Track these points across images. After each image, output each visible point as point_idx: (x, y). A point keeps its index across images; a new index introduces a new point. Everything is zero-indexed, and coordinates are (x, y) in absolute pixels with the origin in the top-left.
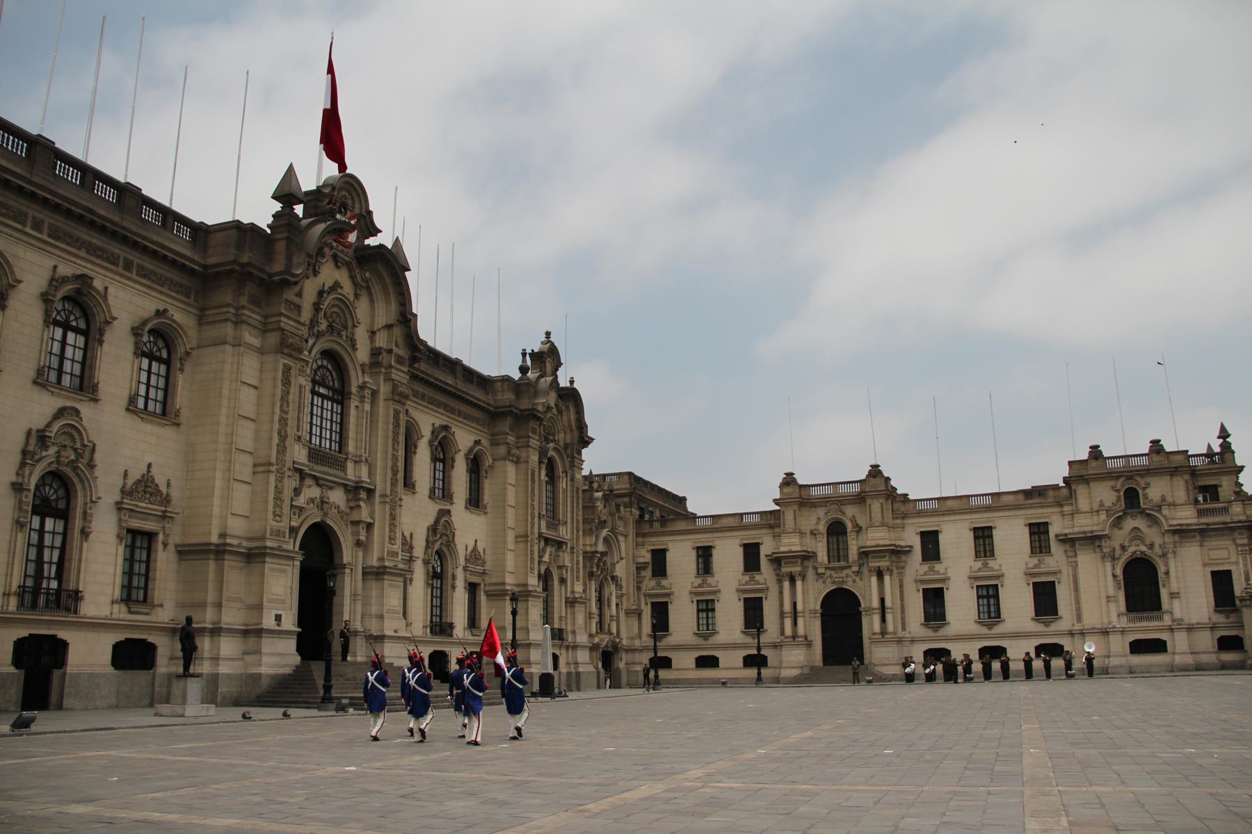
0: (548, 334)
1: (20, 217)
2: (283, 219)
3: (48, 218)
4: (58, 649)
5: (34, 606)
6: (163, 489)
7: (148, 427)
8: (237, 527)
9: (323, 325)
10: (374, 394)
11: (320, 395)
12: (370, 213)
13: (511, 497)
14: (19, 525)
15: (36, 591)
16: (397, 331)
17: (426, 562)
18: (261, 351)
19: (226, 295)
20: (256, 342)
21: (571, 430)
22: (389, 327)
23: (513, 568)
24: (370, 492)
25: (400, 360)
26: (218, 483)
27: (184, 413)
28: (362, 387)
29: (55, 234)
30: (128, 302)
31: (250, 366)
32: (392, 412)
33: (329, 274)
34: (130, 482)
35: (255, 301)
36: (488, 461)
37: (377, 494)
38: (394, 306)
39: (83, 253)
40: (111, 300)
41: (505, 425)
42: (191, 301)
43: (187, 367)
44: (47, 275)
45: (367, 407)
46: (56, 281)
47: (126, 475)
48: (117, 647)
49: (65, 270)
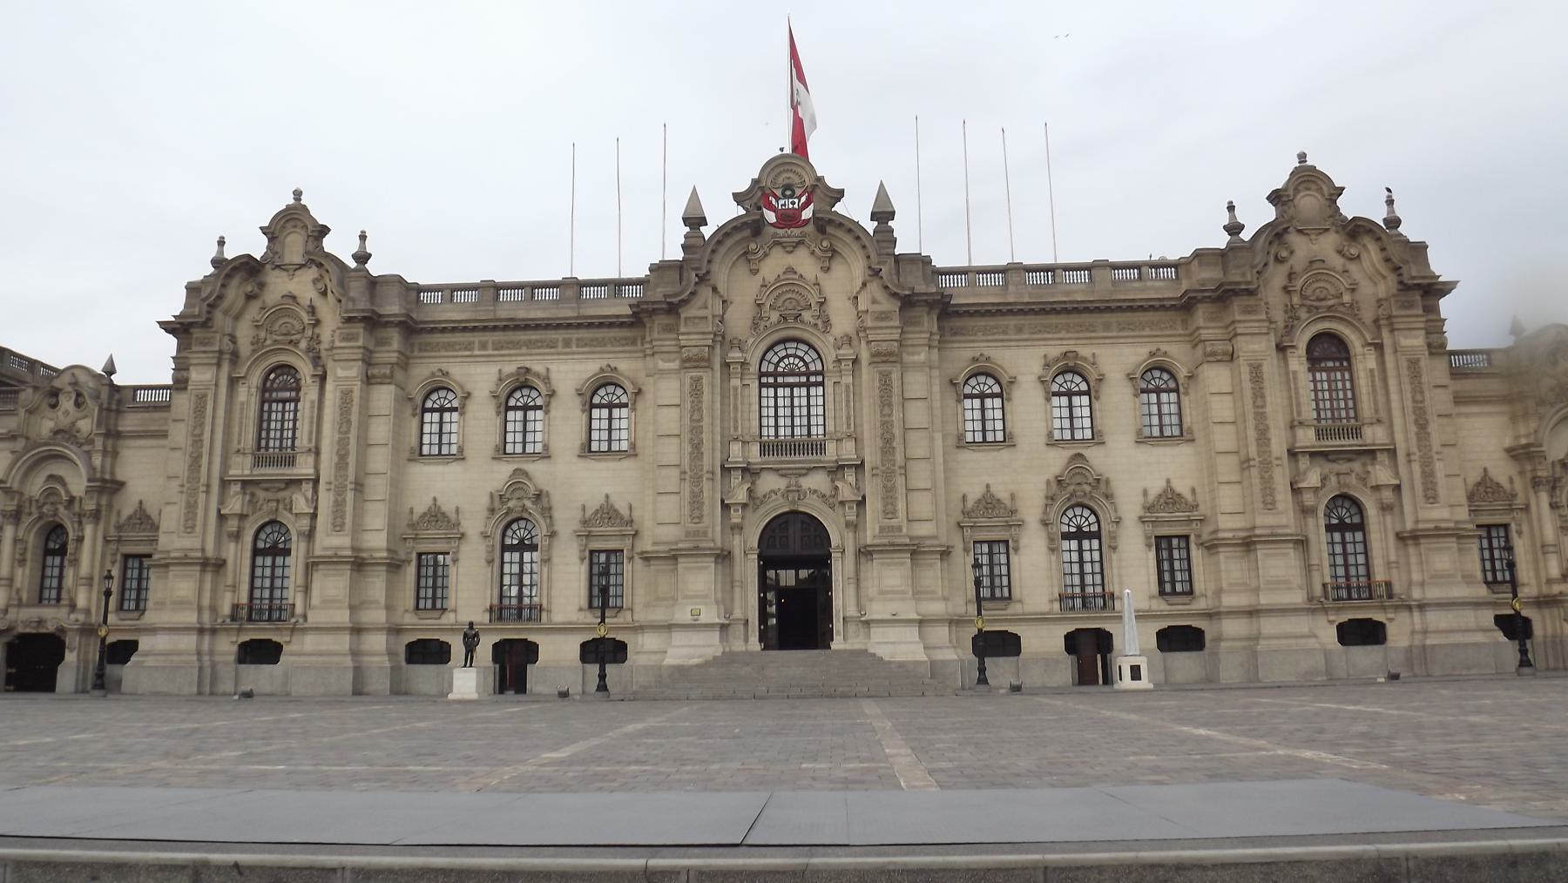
0: (1302, 157)
1: (469, 347)
4: (529, 651)
5: (500, 618)
6: (625, 512)
7: (603, 465)
8: (669, 533)
9: (775, 316)
10: (855, 361)
11: (784, 385)
12: (820, 179)
13: (1223, 408)
14: (490, 562)
15: (501, 609)
16: (874, 287)
17: (1045, 523)
18: (677, 371)
21: (1384, 277)
22: (864, 284)
23: (1229, 510)
24: (860, 467)
25: (883, 316)
27: (639, 443)
28: (839, 361)
30: (569, 372)
32: (877, 376)
33: (774, 265)
34: (589, 513)
36: (1182, 373)
37: (867, 466)
39: (524, 350)
40: (553, 376)
41: (1201, 314)
42: (639, 347)
43: (639, 405)
44: (494, 378)
45: (848, 379)
47: (584, 508)
48: (584, 646)
49: (510, 368)
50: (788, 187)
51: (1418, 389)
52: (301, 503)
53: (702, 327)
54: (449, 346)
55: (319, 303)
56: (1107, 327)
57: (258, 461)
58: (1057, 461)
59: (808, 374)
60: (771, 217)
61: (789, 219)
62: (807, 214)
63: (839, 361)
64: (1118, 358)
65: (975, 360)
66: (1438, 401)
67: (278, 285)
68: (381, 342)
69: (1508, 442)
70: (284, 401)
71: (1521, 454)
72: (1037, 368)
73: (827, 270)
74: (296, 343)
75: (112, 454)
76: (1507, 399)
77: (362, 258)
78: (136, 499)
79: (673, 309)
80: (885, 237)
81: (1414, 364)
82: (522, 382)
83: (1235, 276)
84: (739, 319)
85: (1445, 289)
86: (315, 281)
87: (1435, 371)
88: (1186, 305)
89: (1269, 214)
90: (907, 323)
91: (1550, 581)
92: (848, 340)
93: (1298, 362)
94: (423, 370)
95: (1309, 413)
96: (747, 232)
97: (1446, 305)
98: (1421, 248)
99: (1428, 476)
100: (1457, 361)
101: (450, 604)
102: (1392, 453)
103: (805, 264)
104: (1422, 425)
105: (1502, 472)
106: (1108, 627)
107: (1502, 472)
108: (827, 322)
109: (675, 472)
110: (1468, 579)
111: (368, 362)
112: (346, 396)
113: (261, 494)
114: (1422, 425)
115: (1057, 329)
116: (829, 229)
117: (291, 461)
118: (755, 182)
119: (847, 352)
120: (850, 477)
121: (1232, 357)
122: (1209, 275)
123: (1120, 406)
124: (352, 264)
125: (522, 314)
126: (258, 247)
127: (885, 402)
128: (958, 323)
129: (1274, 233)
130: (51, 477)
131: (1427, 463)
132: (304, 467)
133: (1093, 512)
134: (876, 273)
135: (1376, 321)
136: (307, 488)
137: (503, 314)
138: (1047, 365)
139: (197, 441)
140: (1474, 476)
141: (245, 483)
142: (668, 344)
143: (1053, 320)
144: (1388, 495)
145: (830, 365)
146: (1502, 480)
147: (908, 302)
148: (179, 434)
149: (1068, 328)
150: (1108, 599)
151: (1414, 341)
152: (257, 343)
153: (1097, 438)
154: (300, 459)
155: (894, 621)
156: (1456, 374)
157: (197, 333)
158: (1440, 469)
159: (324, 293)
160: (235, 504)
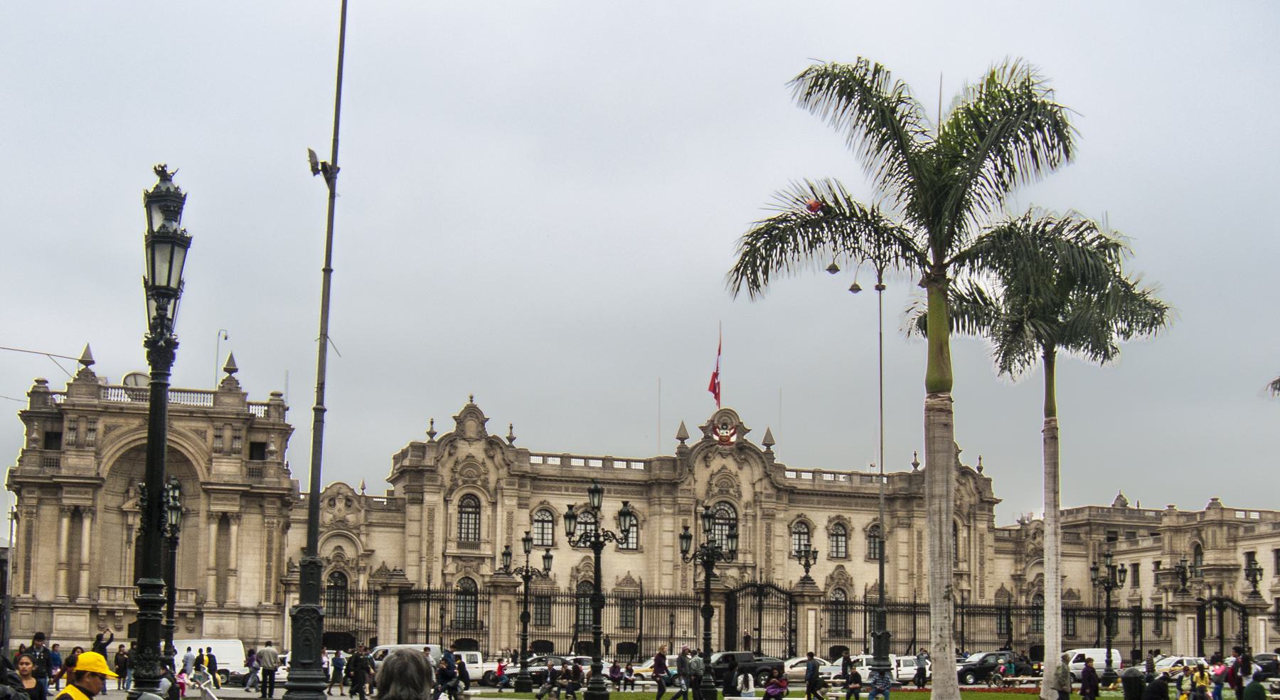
1: (559, 489)
2: (683, 451)
3: (570, 486)
9: (716, 490)
10: (755, 517)
13: (903, 549)
16: (765, 482)
18: (673, 514)
19: (655, 494)
20: (671, 511)
24: (754, 568)
25: (768, 496)
26: (656, 576)
28: (746, 515)
29: (574, 490)
31: (668, 523)
33: (717, 463)
35: (668, 492)
38: (761, 469)
41: (898, 505)
43: (645, 526)
45: (750, 524)
50: (725, 424)
51: (982, 548)
53: (687, 494)
54: (549, 488)
55: (488, 462)
56: (856, 505)
57: (460, 545)
58: (831, 567)
59: (730, 519)
60: (716, 438)
61: (724, 441)
62: (733, 439)
63: (746, 515)
64: (860, 520)
65: (799, 516)
66: (989, 552)
67: (464, 449)
68: (521, 486)
69: (1013, 572)
70: (469, 513)
71: (1017, 578)
72: (825, 523)
73: (740, 468)
74: (474, 482)
75: (367, 535)
76: (1014, 553)
77: (511, 439)
78: (381, 561)
79: (673, 485)
80: (769, 454)
81: (982, 535)
83: (914, 489)
84: (700, 489)
85: (998, 501)
86: (486, 451)
87: (989, 539)
88: (891, 499)
90: (778, 498)
91: (1021, 635)
92: (747, 506)
94: (535, 501)
96: (708, 448)
97: (996, 507)
98: (989, 480)
99: (982, 586)
100: (1000, 534)
101: (553, 622)
102: (969, 575)
103: (731, 464)
104: (982, 564)
105: (1009, 585)
106: (848, 645)
107: (1009, 585)
108: (740, 496)
109: (671, 565)
110: (992, 633)
111: (520, 498)
112: (510, 514)
113: (461, 563)
114: (982, 564)
115: (835, 504)
116: (743, 451)
117: (476, 546)
118: (712, 421)
119: (749, 511)
120: (749, 571)
121: (909, 526)
122: (901, 485)
123: (859, 544)
124: (507, 443)
125: (586, 475)
126: (452, 427)
127: (768, 538)
128: (794, 497)
130: (339, 547)
131: (982, 581)
132: (486, 550)
133: (844, 592)
134: (767, 475)
135: (969, 514)
136: (488, 561)
137: (577, 473)
138: (830, 521)
139: (431, 534)
140: (998, 586)
141: (455, 558)
142: (669, 500)
143: (834, 499)
144: (966, 594)
145: (741, 517)
146: (1008, 589)
147: (779, 490)
148: (413, 528)
149: (840, 504)
150: (848, 633)
151: (982, 526)
152: (453, 480)
153: (847, 557)
154: (482, 546)
155: (770, 640)
156: (997, 539)
157: (427, 475)
158: (987, 584)
159: (492, 458)
160: (451, 568)
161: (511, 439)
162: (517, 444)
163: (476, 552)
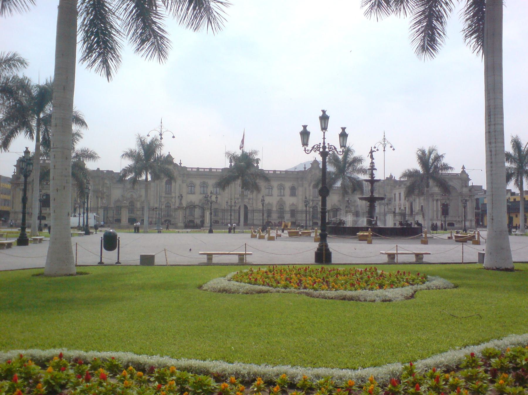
23: (301, 206)
24: (253, 199)
46: (201, 183)
52: (173, 200)
58: (279, 198)
77: (180, 164)
82: (204, 183)
89: (310, 166)
93: (311, 188)
95: (312, 194)
112: (180, 185)
117: (171, 194)
121: (303, 186)
123: (287, 191)
129: (310, 169)
150: (283, 218)
153: (284, 196)
160: (163, 200)
161: (180, 164)
162: (182, 165)
163: (169, 196)
